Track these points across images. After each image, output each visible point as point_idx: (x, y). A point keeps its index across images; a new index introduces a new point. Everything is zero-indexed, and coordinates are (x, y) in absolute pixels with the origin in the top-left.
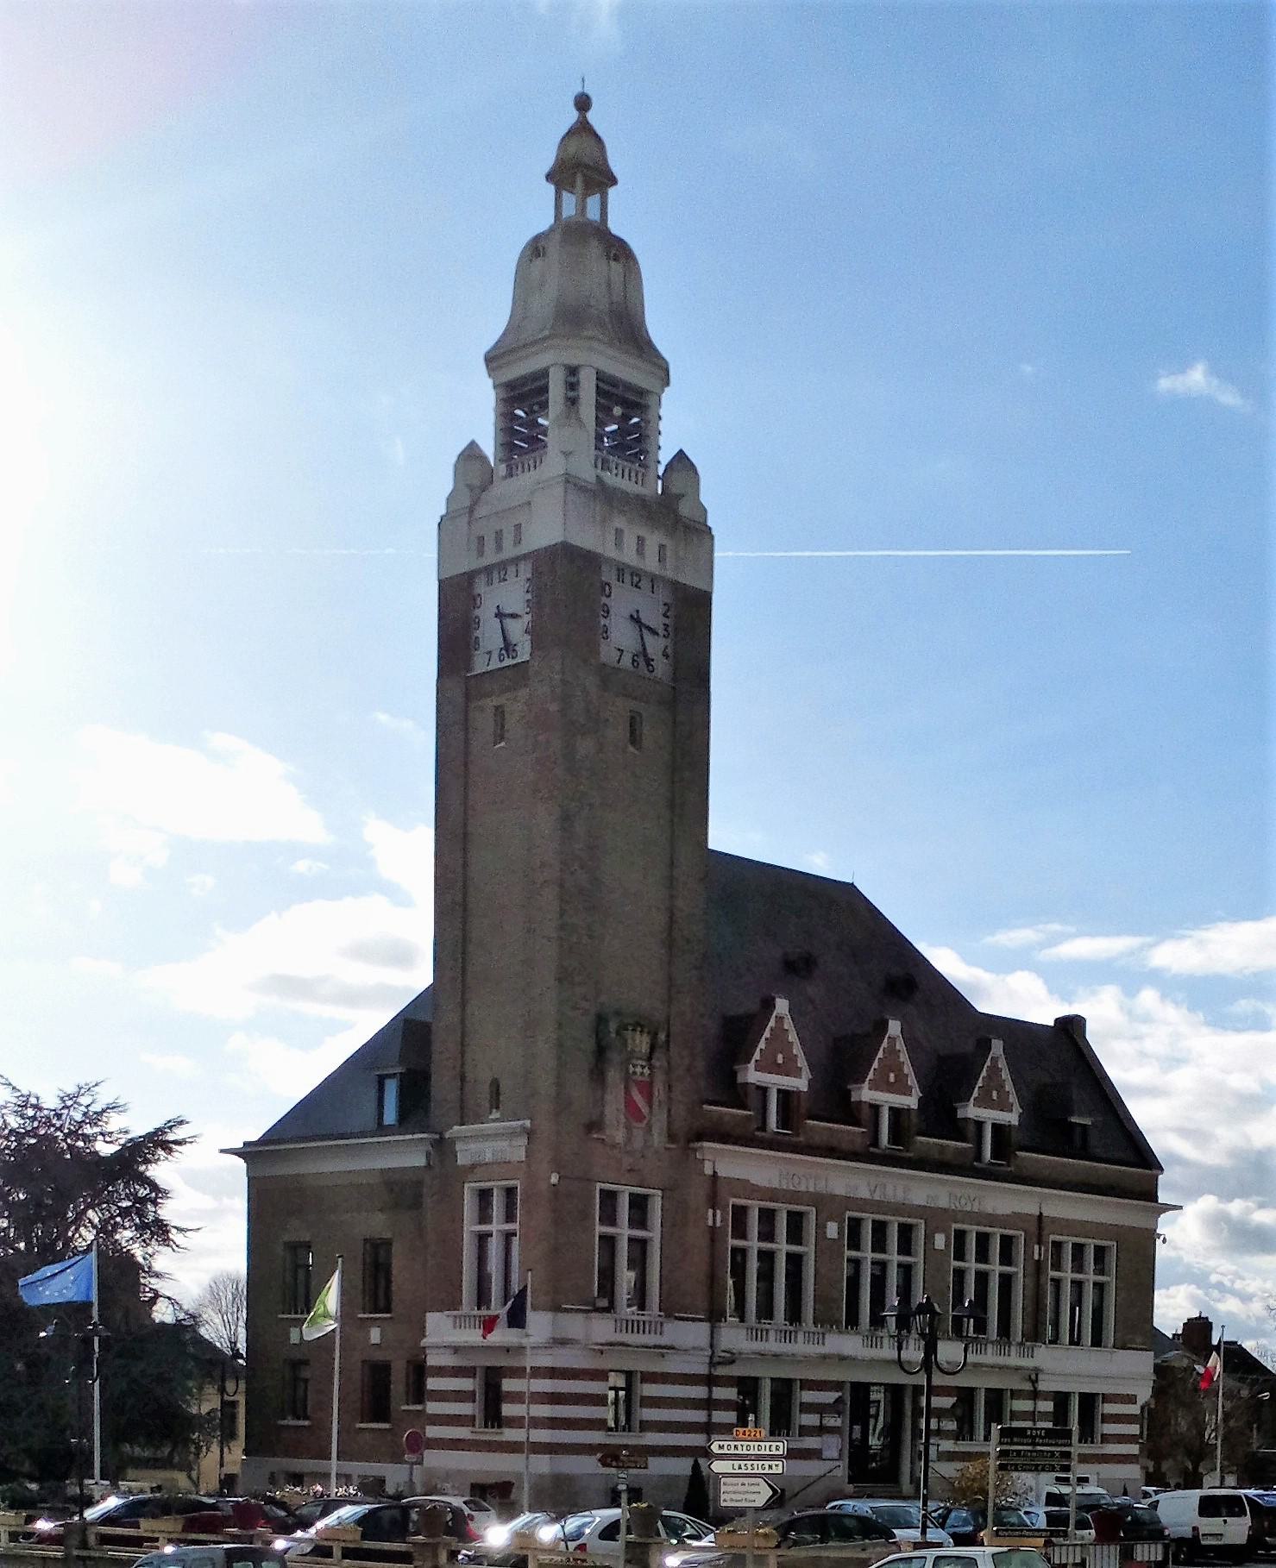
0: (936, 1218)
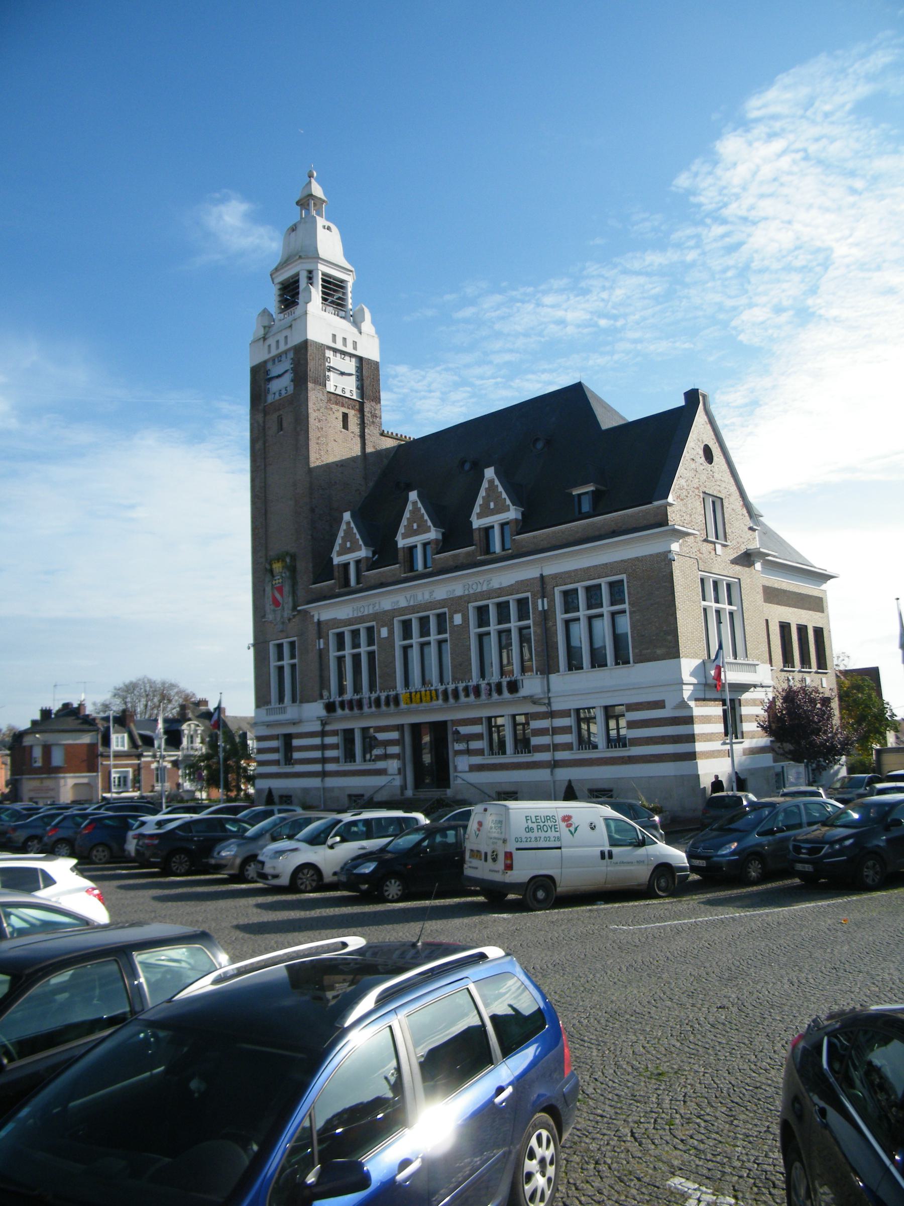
0: (458, 604)
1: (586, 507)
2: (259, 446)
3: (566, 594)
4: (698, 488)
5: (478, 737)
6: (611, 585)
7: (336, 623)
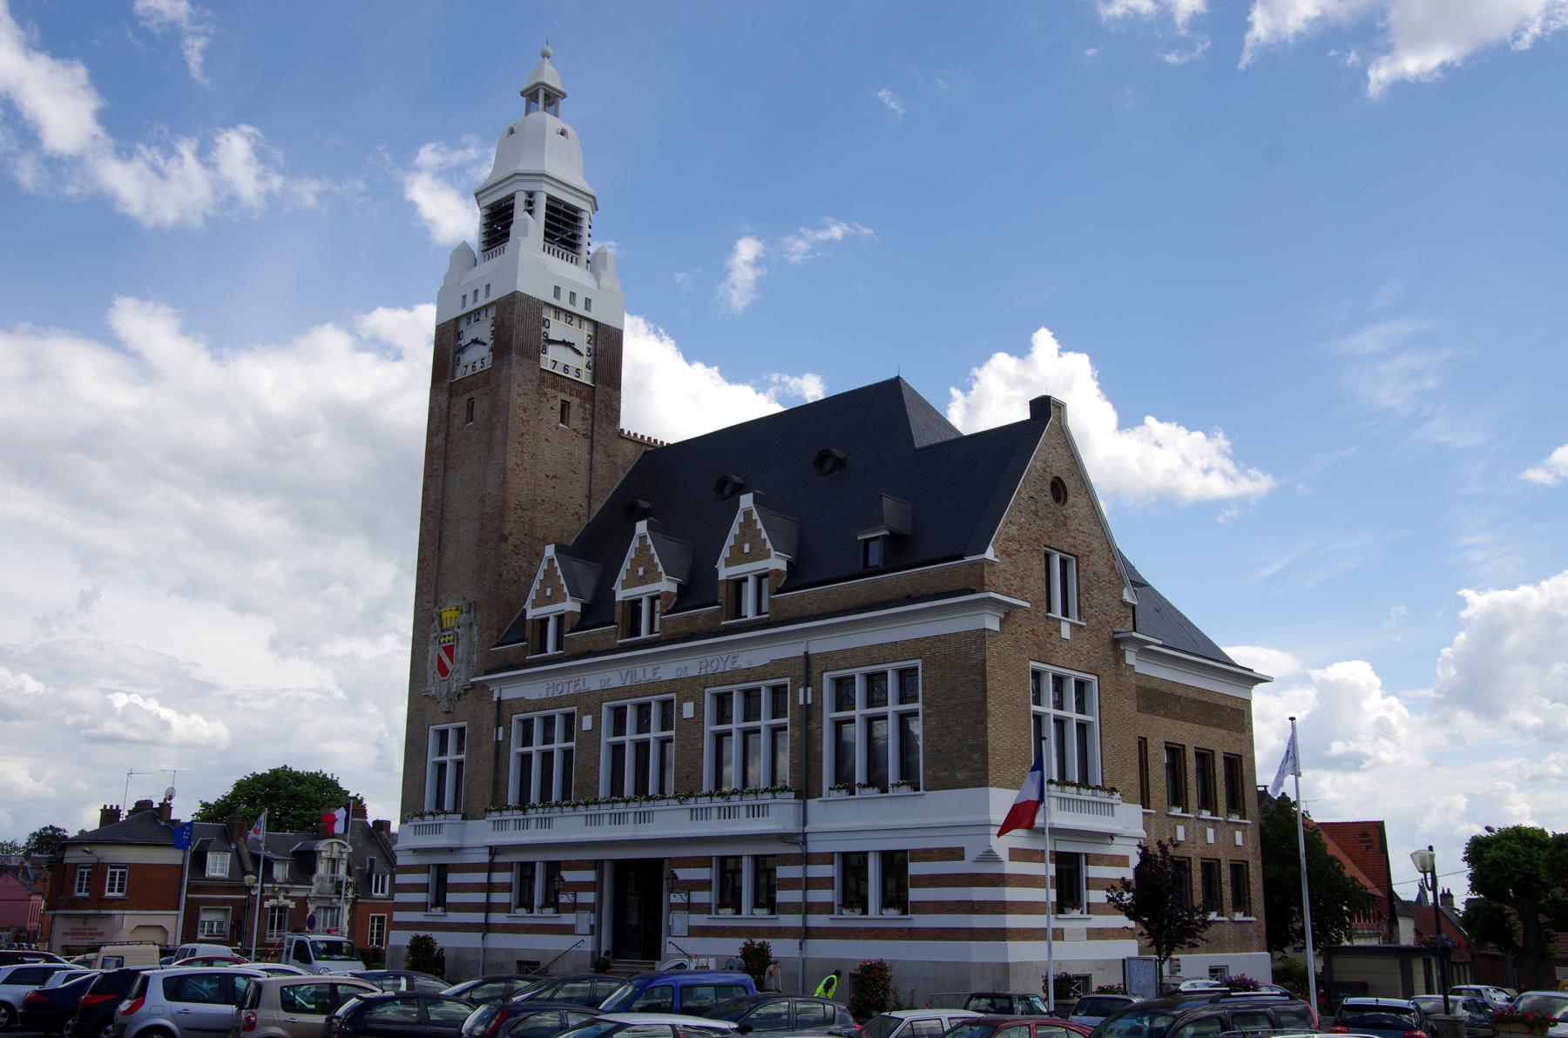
0: (689, 687)
1: (875, 559)
2: (439, 440)
3: (839, 682)
4: (1036, 540)
5: (704, 885)
6: (902, 673)
7: (523, 704)
